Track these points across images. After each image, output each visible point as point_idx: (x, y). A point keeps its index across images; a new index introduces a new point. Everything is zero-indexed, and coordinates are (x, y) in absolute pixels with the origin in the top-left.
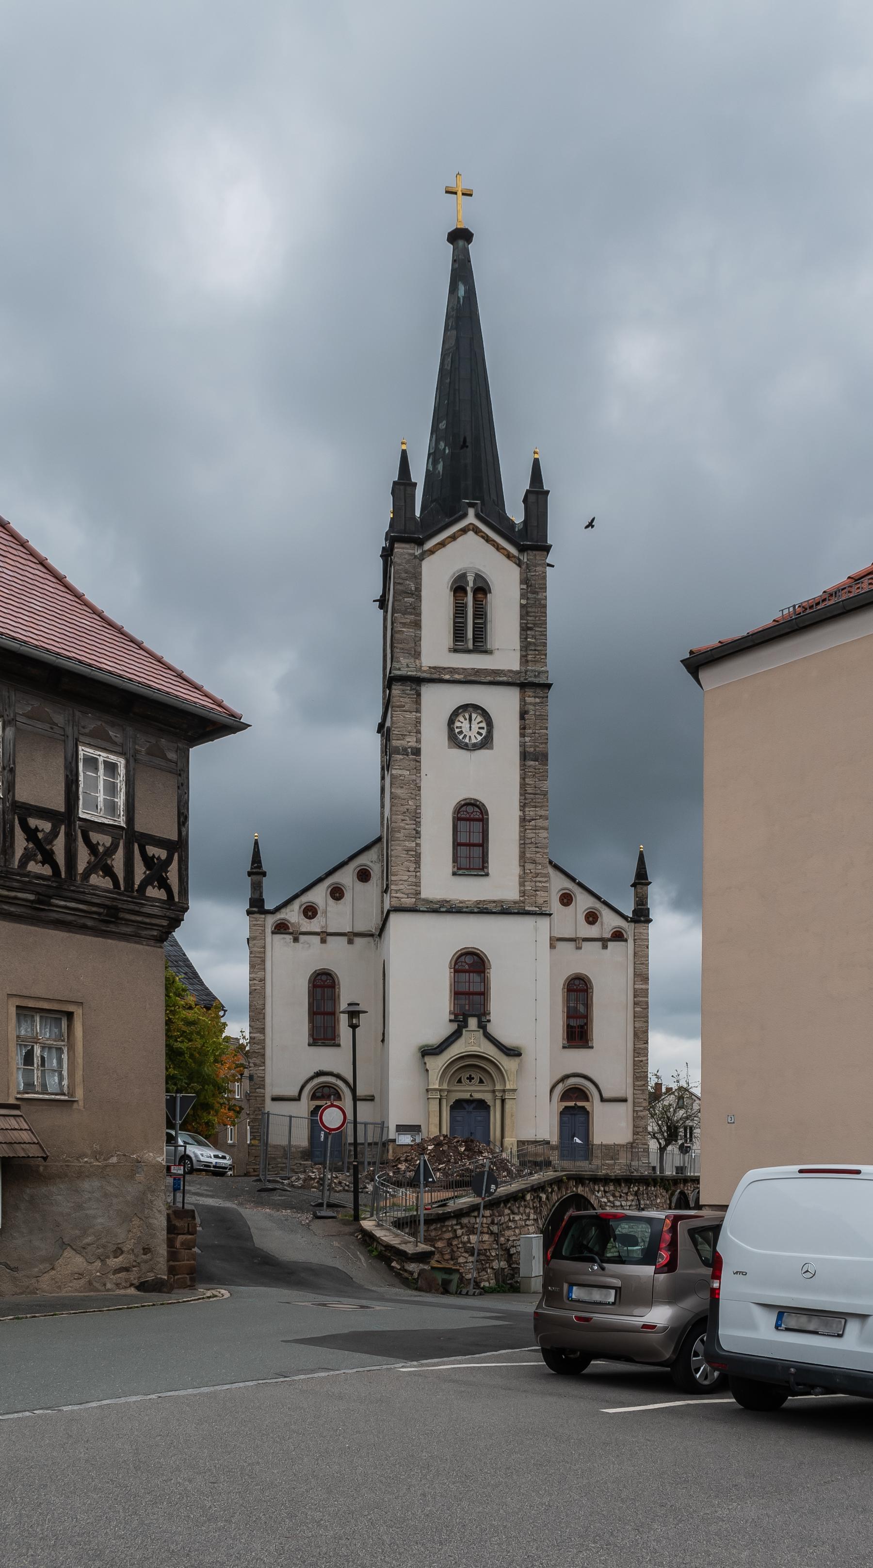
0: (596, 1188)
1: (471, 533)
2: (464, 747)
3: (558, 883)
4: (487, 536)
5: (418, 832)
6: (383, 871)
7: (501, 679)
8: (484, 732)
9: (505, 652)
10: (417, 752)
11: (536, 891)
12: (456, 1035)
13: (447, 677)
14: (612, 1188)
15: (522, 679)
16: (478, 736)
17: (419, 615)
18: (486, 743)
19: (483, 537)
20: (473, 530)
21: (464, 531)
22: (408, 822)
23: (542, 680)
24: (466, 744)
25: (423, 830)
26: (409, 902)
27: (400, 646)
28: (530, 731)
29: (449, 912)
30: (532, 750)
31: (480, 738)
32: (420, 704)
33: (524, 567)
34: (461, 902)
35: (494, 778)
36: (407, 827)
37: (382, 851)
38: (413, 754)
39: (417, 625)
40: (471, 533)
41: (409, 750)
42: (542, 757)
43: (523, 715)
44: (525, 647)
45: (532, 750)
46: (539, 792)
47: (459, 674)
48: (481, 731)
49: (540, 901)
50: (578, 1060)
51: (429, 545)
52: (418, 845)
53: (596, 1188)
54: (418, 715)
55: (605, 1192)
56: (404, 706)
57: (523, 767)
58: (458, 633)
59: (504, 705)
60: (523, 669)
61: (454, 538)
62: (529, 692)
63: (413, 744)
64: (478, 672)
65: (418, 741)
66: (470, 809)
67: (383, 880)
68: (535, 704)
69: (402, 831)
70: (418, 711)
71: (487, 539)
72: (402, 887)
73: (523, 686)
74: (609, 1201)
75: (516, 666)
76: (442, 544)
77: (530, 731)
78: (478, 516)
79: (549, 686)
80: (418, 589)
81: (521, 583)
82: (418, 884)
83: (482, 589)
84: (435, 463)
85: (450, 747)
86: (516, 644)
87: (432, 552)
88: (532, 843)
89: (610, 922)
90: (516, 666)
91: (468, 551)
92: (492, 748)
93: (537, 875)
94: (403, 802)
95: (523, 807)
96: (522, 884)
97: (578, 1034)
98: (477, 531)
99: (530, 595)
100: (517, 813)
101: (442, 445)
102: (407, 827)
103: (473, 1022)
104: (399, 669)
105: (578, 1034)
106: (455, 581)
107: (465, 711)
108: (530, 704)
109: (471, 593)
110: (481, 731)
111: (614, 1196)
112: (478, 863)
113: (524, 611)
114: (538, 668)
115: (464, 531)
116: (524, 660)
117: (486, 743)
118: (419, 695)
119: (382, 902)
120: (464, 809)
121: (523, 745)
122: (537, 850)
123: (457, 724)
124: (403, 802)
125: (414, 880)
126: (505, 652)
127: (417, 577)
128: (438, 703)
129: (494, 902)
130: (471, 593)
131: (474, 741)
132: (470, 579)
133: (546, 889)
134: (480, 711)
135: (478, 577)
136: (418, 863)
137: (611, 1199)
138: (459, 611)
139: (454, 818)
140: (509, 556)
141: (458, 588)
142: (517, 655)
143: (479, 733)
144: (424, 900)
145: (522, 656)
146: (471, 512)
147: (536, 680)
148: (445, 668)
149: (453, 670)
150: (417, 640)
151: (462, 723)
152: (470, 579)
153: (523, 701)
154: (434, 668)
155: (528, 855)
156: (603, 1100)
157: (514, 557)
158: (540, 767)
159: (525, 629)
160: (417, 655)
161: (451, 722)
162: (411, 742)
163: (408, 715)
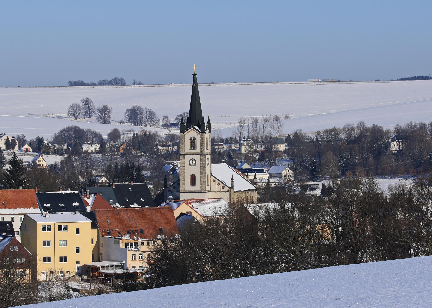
10: (184, 167)
18: (195, 164)
43: (201, 160)
44: (201, 149)
58: (191, 147)
59: (198, 158)
64: (195, 153)
73: (201, 155)
83: (195, 139)
86: (200, 148)
113: (201, 143)
126: (198, 150)
128: (187, 158)
138: (191, 143)
141: (191, 139)
142: (200, 150)
159: (201, 146)
161: (189, 161)
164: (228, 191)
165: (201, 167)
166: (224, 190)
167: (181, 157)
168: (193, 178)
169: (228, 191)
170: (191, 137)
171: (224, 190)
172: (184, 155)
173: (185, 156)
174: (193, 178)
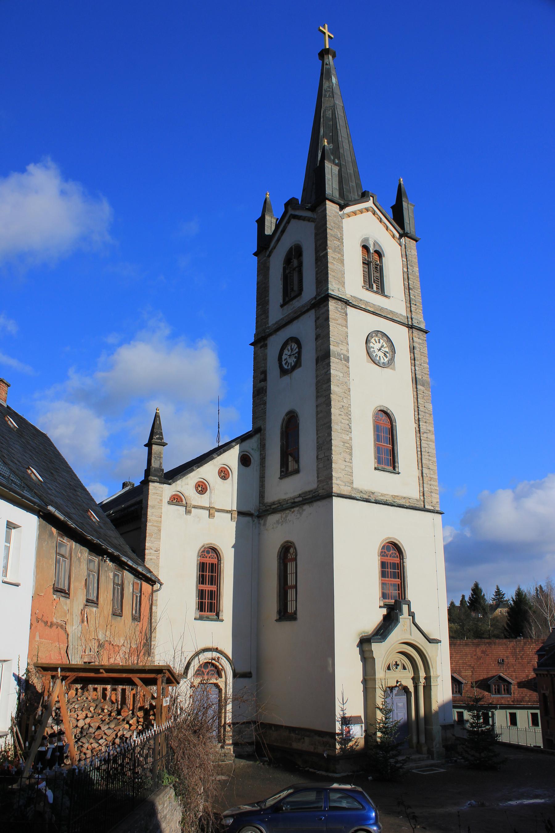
1: (370, 213)
4: (381, 219)
7: (396, 319)
11: (431, 492)
17: (343, 256)
19: (378, 219)
20: (372, 212)
21: (367, 210)
22: (343, 417)
25: (353, 425)
26: (345, 490)
29: (377, 502)
30: (420, 377)
31: (386, 360)
33: (403, 246)
36: (343, 421)
38: (345, 361)
45: (420, 377)
46: (427, 411)
47: (370, 307)
52: (351, 439)
56: (337, 320)
62: (416, 332)
68: (419, 344)
69: (340, 424)
72: (341, 475)
73: (411, 327)
76: (355, 213)
82: (351, 474)
85: (368, 362)
88: (425, 451)
92: (394, 369)
94: (340, 399)
100: (414, 425)
102: (343, 421)
104: (333, 291)
115: (367, 210)
118: (347, 314)
122: (430, 458)
123: (371, 345)
124: (340, 399)
127: (340, 228)
129: (404, 498)
134: (385, 339)
136: (351, 454)
140: (393, 236)
144: (356, 489)
148: (361, 300)
149: (367, 303)
151: (375, 345)
153: (412, 340)
155: (423, 461)
160: (343, 284)
165: (416, 381)
167: (332, 305)
168: (385, 426)
170: (366, 240)
172: (347, 303)
173: (350, 310)
174: (385, 426)
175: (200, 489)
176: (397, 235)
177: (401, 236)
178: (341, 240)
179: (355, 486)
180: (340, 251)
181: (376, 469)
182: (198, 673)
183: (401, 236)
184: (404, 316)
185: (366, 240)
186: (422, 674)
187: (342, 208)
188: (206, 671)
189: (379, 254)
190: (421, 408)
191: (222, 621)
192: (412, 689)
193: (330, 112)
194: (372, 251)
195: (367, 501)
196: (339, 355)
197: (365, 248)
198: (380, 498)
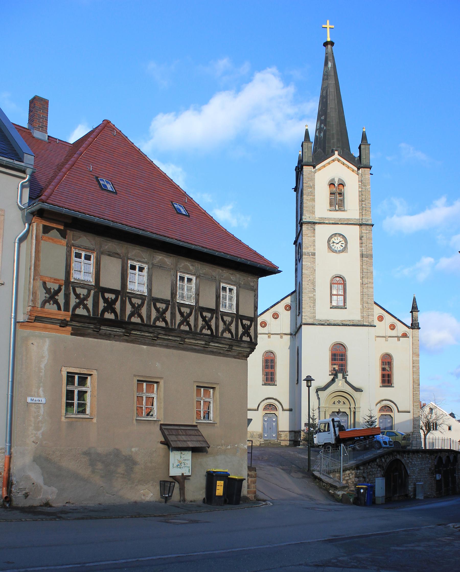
0: (405, 455)
1: (336, 162)
2: (335, 252)
3: (378, 311)
5: (314, 290)
6: (296, 306)
8: (344, 245)
9: (352, 210)
10: (314, 254)
12: (333, 381)
13: (327, 222)
14: (411, 455)
15: (361, 223)
16: (341, 247)
18: (345, 250)
21: (333, 161)
23: (369, 222)
24: (336, 251)
25: (316, 288)
26: (310, 321)
27: (307, 209)
28: (365, 245)
29: (328, 325)
30: (365, 253)
31: (342, 248)
32: (315, 234)
34: (334, 321)
35: (348, 265)
37: (296, 296)
38: (312, 255)
39: (313, 200)
40: (336, 162)
41: (310, 254)
42: (370, 256)
43: (361, 238)
44: (362, 209)
46: (369, 271)
48: (342, 245)
49: (370, 320)
50: (387, 393)
51: (317, 167)
52: (314, 295)
53: (405, 455)
54: (314, 238)
55: (408, 457)
57: (362, 261)
60: (361, 218)
61: (329, 163)
62: (364, 227)
63: (312, 251)
64: (340, 219)
65: (314, 249)
66: (338, 279)
67: (297, 309)
70: (314, 236)
71: (344, 164)
72: (307, 314)
73: (360, 225)
74: (410, 462)
75: (357, 217)
76: (324, 166)
77: (365, 245)
78: (338, 155)
79: (373, 225)
80: (314, 185)
81: (359, 182)
82: (314, 313)
84: (320, 133)
85: (328, 252)
87: (320, 169)
89: (401, 329)
90: (357, 217)
91: (335, 168)
93: (369, 309)
95: (362, 278)
96: (362, 313)
97: (387, 380)
98: (339, 161)
99: (363, 187)
100: (359, 281)
101: (323, 126)
103: (340, 375)
105: (387, 380)
106: (330, 181)
107: (335, 236)
108: (364, 233)
109: (337, 192)
110: (342, 245)
111: (412, 459)
112: (341, 304)
114: (367, 217)
115: (333, 161)
116: (361, 214)
117: (345, 250)
118: (315, 230)
119: (296, 319)
120: (335, 279)
121: (361, 251)
125: (313, 311)
126: (352, 210)
127: (313, 180)
128: (322, 232)
130: (337, 192)
131: (339, 249)
132: (336, 180)
133: (373, 315)
134: (341, 236)
135: (340, 180)
136: (314, 303)
137: (411, 461)
139: (331, 283)
140: (353, 171)
143: (342, 246)
145: (360, 213)
146: (336, 153)
147: (367, 223)
149: (329, 219)
150: (313, 207)
152: (336, 180)
153: (361, 232)
154: (321, 218)
155: (364, 300)
156: (398, 412)
157: (355, 171)
158: (370, 260)
159: (361, 201)
160: (313, 213)
162: (311, 250)
163: (310, 238)
164: (405, 335)
165: (362, 256)
166: (393, 333)
167: (305, 227)
169: (405, 335)
170: (333, 179)
171: (393, 333)
172: (314, 223)
173: (317, 226)
175: (263, 325)
176: (356, 169)
177: (359, 169)
178: (313, 187)
179: (317, 318)
180: (312, 194)
181: (331, 308)
182: (265, 409)
183: (359, 169)
184: (357, 219)
185: (333, 179)
186: (353, 406)
187: (314, 167)
188: (270, 408)
189: (342, 184)
190: (365, 271)
191: (276, 385)
192: (349, 413)
193: (325, 92)
194: (336, 186)
195: (322, 325)
196: (308, 253)
197: (332, 184)
198: (333, 322)
